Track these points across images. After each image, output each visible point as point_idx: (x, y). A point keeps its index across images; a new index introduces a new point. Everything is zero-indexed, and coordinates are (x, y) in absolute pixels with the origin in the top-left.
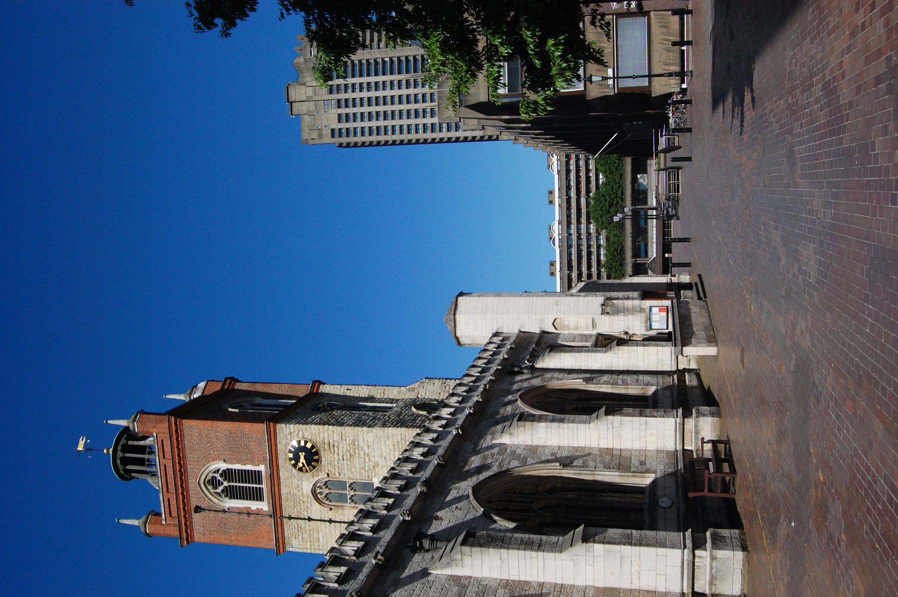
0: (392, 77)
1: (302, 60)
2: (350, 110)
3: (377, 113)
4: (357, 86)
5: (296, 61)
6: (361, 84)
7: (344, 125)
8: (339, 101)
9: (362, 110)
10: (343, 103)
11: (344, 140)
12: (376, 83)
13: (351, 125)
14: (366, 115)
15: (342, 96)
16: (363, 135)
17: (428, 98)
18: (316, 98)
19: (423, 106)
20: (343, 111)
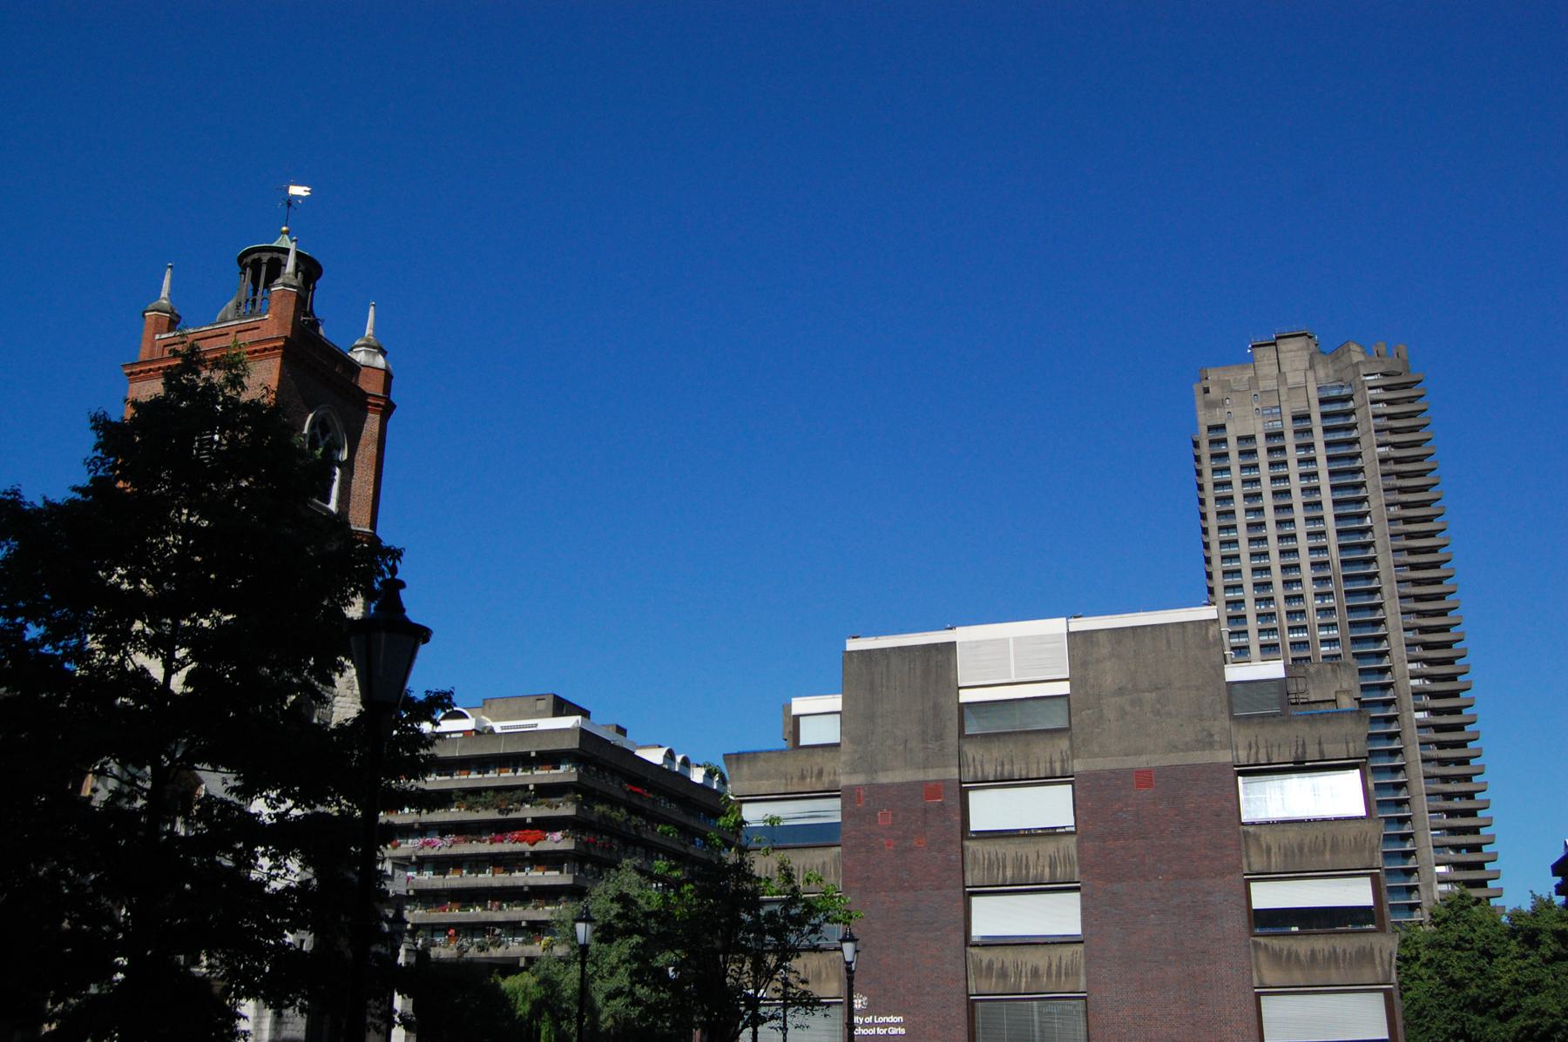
0: (1332, 534)
1: (1357, 357)
2: (1263, 458)
3: (1260, 510)
4: (1311, 468)
5: (1353, 347)
6: (1315, 475)
7: (1233, 448)
8: (1280, 435)
9: (1265, 480)
10: (1277, 443)
11: (1205, 451)
12: (1318, 504)
13: (1234, 461)
14: (1256, 489)
15: (1290, 441)
16: (1217, 485)
17: (1296, 606)
18: (1283, 391)
19: (1280, 598)
20: (1261, 445)
